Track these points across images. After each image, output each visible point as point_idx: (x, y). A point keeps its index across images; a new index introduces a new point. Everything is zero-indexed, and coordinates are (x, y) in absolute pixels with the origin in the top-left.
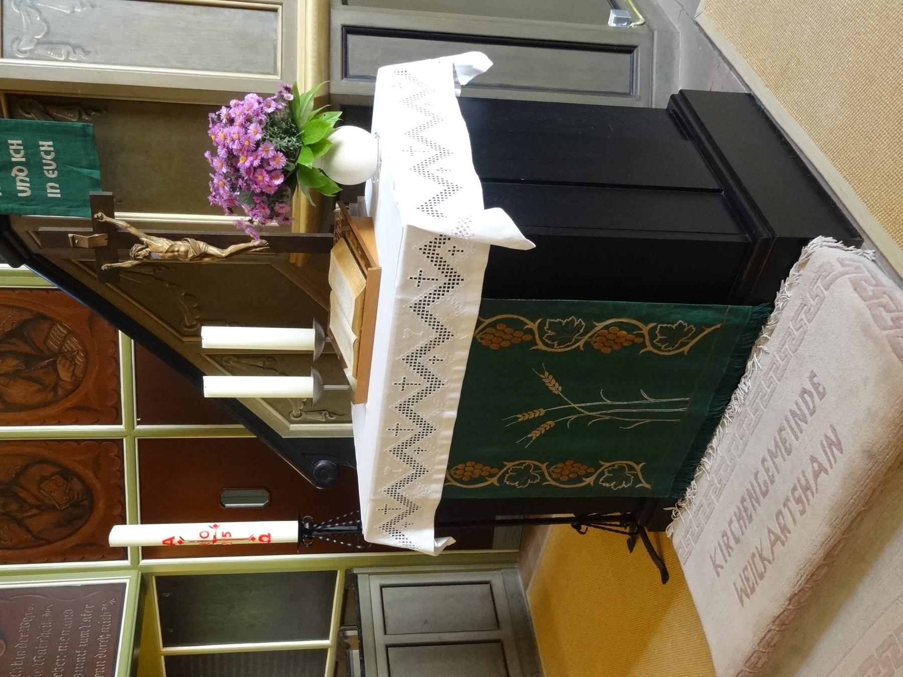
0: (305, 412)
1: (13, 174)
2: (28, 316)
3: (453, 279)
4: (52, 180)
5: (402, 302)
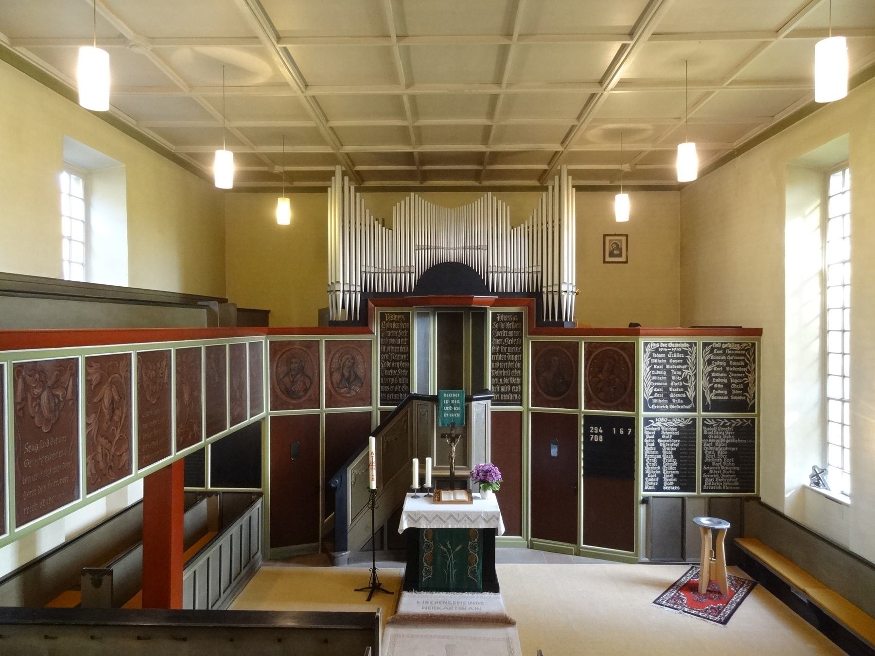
2: (362, 380)
3: (487, 522)
5: (481, 512)
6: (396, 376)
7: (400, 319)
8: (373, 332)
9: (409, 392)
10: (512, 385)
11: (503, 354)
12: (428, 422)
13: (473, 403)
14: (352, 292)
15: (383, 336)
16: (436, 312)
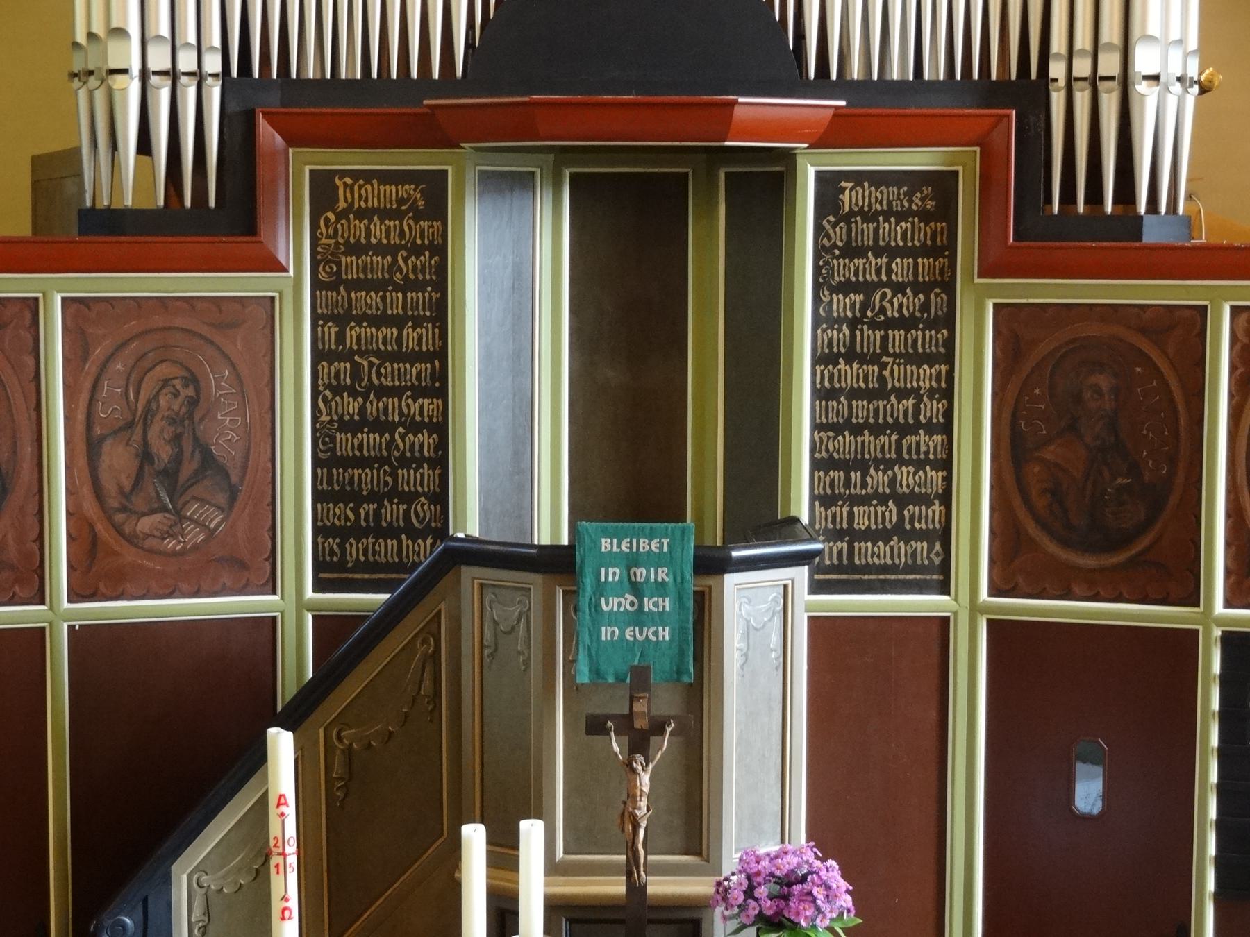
0: (206, 894)
1: (627, 596)
2: (234, 479)
4: (622, 632)
6: (382, 461)
7: (401, 201)
8: (284, 263)
9: (442, 532)
10: (902, 501)
11: (863, 359)
12: (527, 663)
13: (732, 580)
14: (184, 80)
15: (322, 276)
16: (567, 173)
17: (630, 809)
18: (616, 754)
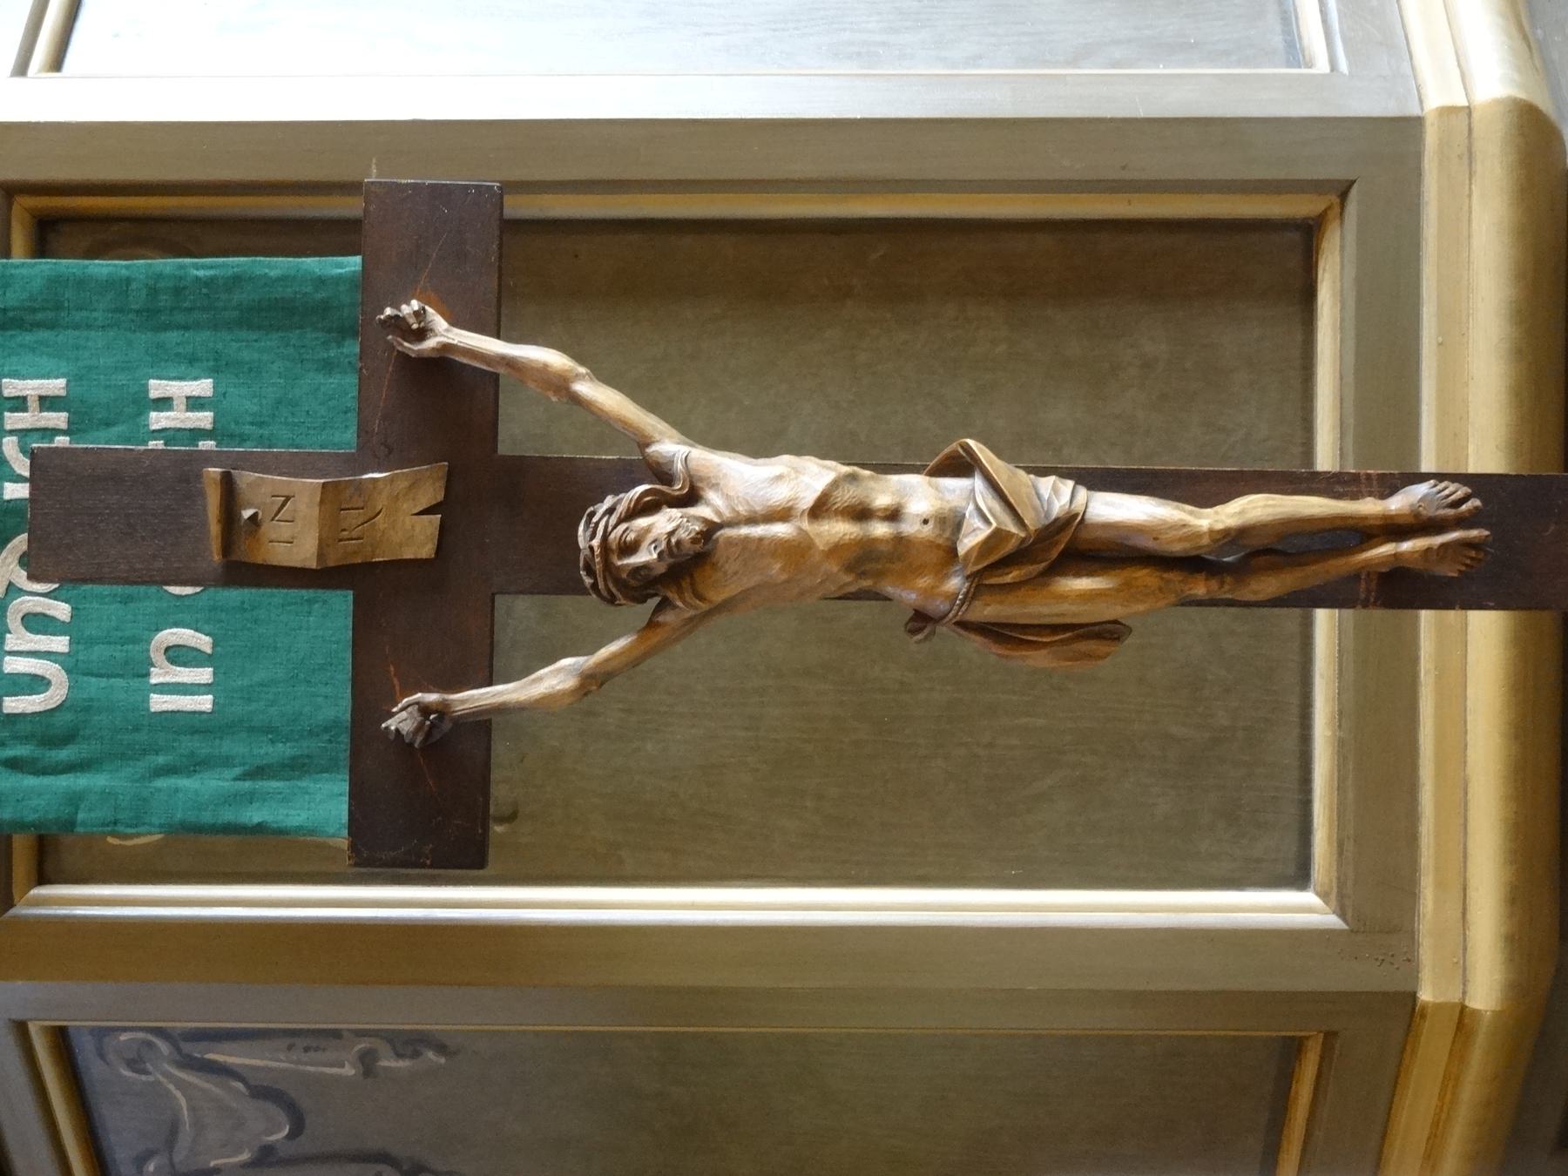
12: (410, 1043)
17: (955, 583)
18: (591, 682)
